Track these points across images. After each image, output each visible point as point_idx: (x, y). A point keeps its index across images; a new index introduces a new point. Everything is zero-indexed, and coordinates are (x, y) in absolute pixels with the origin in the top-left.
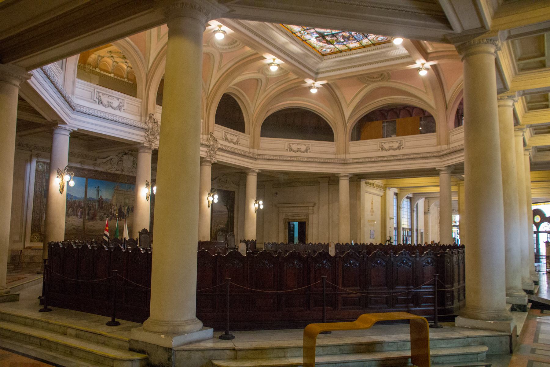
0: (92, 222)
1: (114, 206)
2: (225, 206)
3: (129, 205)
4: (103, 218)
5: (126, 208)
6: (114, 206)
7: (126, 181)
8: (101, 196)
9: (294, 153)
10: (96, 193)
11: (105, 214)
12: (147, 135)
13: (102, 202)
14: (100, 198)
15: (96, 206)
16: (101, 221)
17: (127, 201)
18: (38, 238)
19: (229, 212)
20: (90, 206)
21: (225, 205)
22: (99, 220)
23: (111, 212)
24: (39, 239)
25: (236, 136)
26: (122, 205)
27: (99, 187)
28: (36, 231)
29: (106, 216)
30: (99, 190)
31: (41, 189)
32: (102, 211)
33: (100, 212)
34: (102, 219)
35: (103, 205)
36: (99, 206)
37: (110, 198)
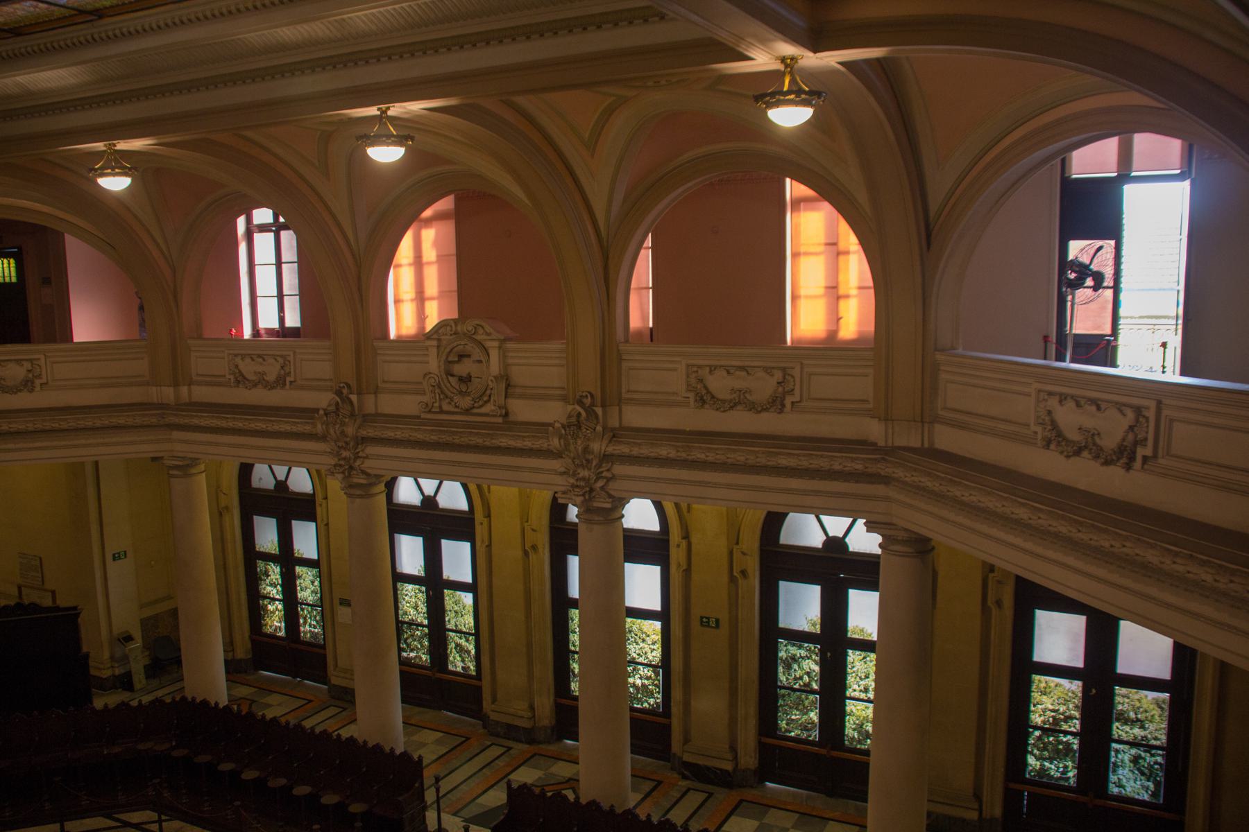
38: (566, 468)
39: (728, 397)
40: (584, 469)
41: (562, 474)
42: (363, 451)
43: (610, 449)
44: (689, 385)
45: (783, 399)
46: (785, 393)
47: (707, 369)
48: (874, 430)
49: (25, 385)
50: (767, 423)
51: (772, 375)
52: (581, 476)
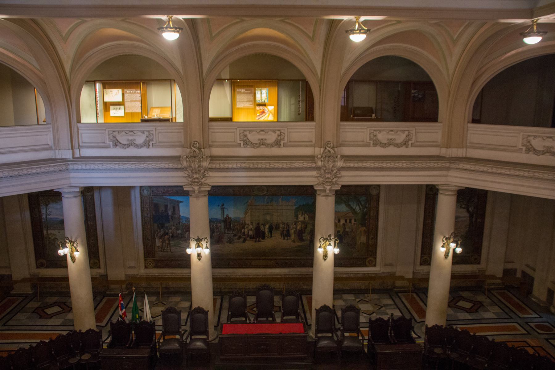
0: (219, 246)
1: (248, 225)
2: (464, 208)
3: (271, 222)
4: (233, 241)
5: (267, 226)
6: (248, 225)
7: (265, 193)
8: (227, 216)
9: (534, 156)
10: (220, 212)
11: (235, 235)
12: (187, 175)
13: (230, 222)
14: (226, 218)
15: (221, 226)
16: (230, 243)
17: (268, 218)
18: (152, 263)
19: (471, 216)
20: (213, 228)
21: (463, 206)
22: (227, 242)
23: (244, 232)
24: (154, 265)
25: (403, 131)
26: (261, 223)
27: (223, 205)
28: (150, 257)
29: (237, 237)
30: (224, 208)
31: (149, 215)
32: (230, 232)
33: (227, 234)
34: (230, 241)
35: (232, 225)
36: (225, 227)
37: (241, 216)
38: (320, 174)
39: (386, 142)
40: (328, 174)
41: (317, 177)
42: (207, 174)
43: (344, 165)
44: (370, 138)
45: (280, 142)
46: (281, 140)
47: (248, 132)
48: (443, 152)
49: (405, 144)
50: (403, 151)
51: (144, 134)
52: (326, 177)
